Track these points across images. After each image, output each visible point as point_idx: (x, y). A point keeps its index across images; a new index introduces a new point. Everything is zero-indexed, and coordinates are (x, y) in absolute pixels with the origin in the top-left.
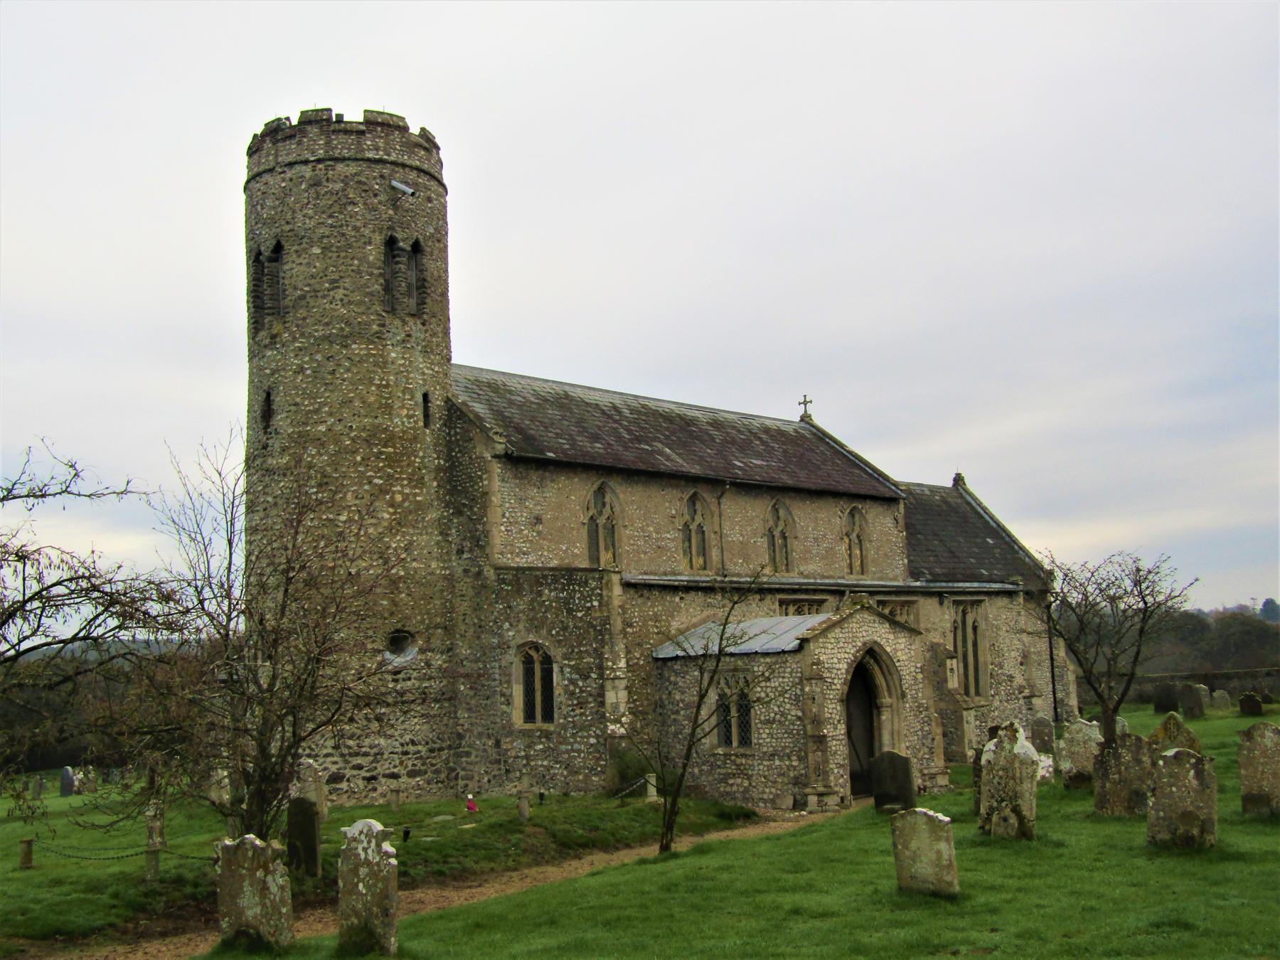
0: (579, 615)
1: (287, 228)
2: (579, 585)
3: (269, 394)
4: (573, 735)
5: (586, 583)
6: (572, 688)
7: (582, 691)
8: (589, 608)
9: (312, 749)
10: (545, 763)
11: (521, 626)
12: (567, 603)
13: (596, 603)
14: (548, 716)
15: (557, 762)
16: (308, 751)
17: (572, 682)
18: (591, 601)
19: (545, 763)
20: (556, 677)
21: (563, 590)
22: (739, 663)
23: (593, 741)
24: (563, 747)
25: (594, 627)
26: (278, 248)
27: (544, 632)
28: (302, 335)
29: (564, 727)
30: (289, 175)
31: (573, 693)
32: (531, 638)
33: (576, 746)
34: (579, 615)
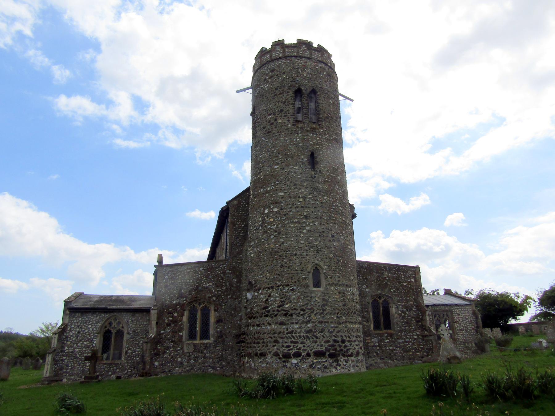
0: (405, 284)
1: (320, 86)
2: (404, 272)
3: (312, 155)
4: (406, 335)
5: (407, 272)
6: (403, 314)
7: (408, 316)
8: (409, 282)
9: (349, 337)
10: (391, 348)
11: (373, 287)
12: (397, 279)
13: (413, 280)
14: (388, 326)
15: (397, 348)
16: (348, 339)
17: (403, 312)
18: (410, 279)
19: (391, 348)
20: (393, 310)
21: (395, 274)
22: (447, 308)
23: (416, 337)
24: (400, 341)
25: (413, 290)
26: (314, 91)
27: (387, 290)
28: (328, 134)
29: (401, 331)
30: (320, 65)
31: (404, 317)
32: (379, 292)
33: (407, 340)
34: (405, 284)
